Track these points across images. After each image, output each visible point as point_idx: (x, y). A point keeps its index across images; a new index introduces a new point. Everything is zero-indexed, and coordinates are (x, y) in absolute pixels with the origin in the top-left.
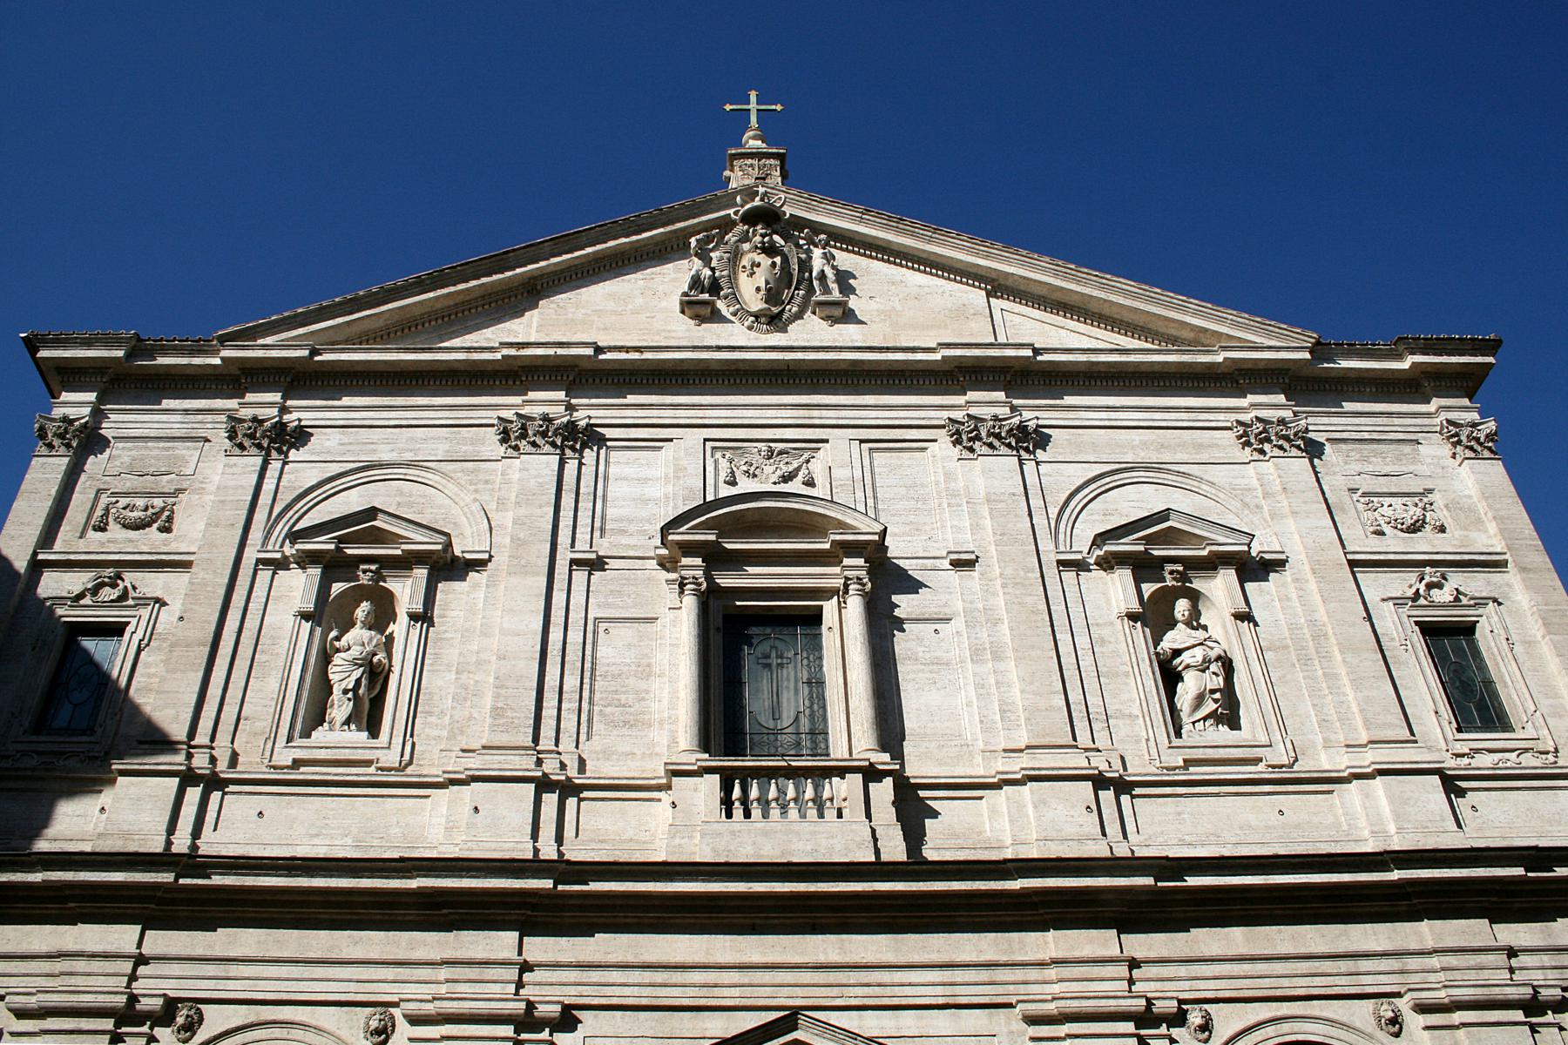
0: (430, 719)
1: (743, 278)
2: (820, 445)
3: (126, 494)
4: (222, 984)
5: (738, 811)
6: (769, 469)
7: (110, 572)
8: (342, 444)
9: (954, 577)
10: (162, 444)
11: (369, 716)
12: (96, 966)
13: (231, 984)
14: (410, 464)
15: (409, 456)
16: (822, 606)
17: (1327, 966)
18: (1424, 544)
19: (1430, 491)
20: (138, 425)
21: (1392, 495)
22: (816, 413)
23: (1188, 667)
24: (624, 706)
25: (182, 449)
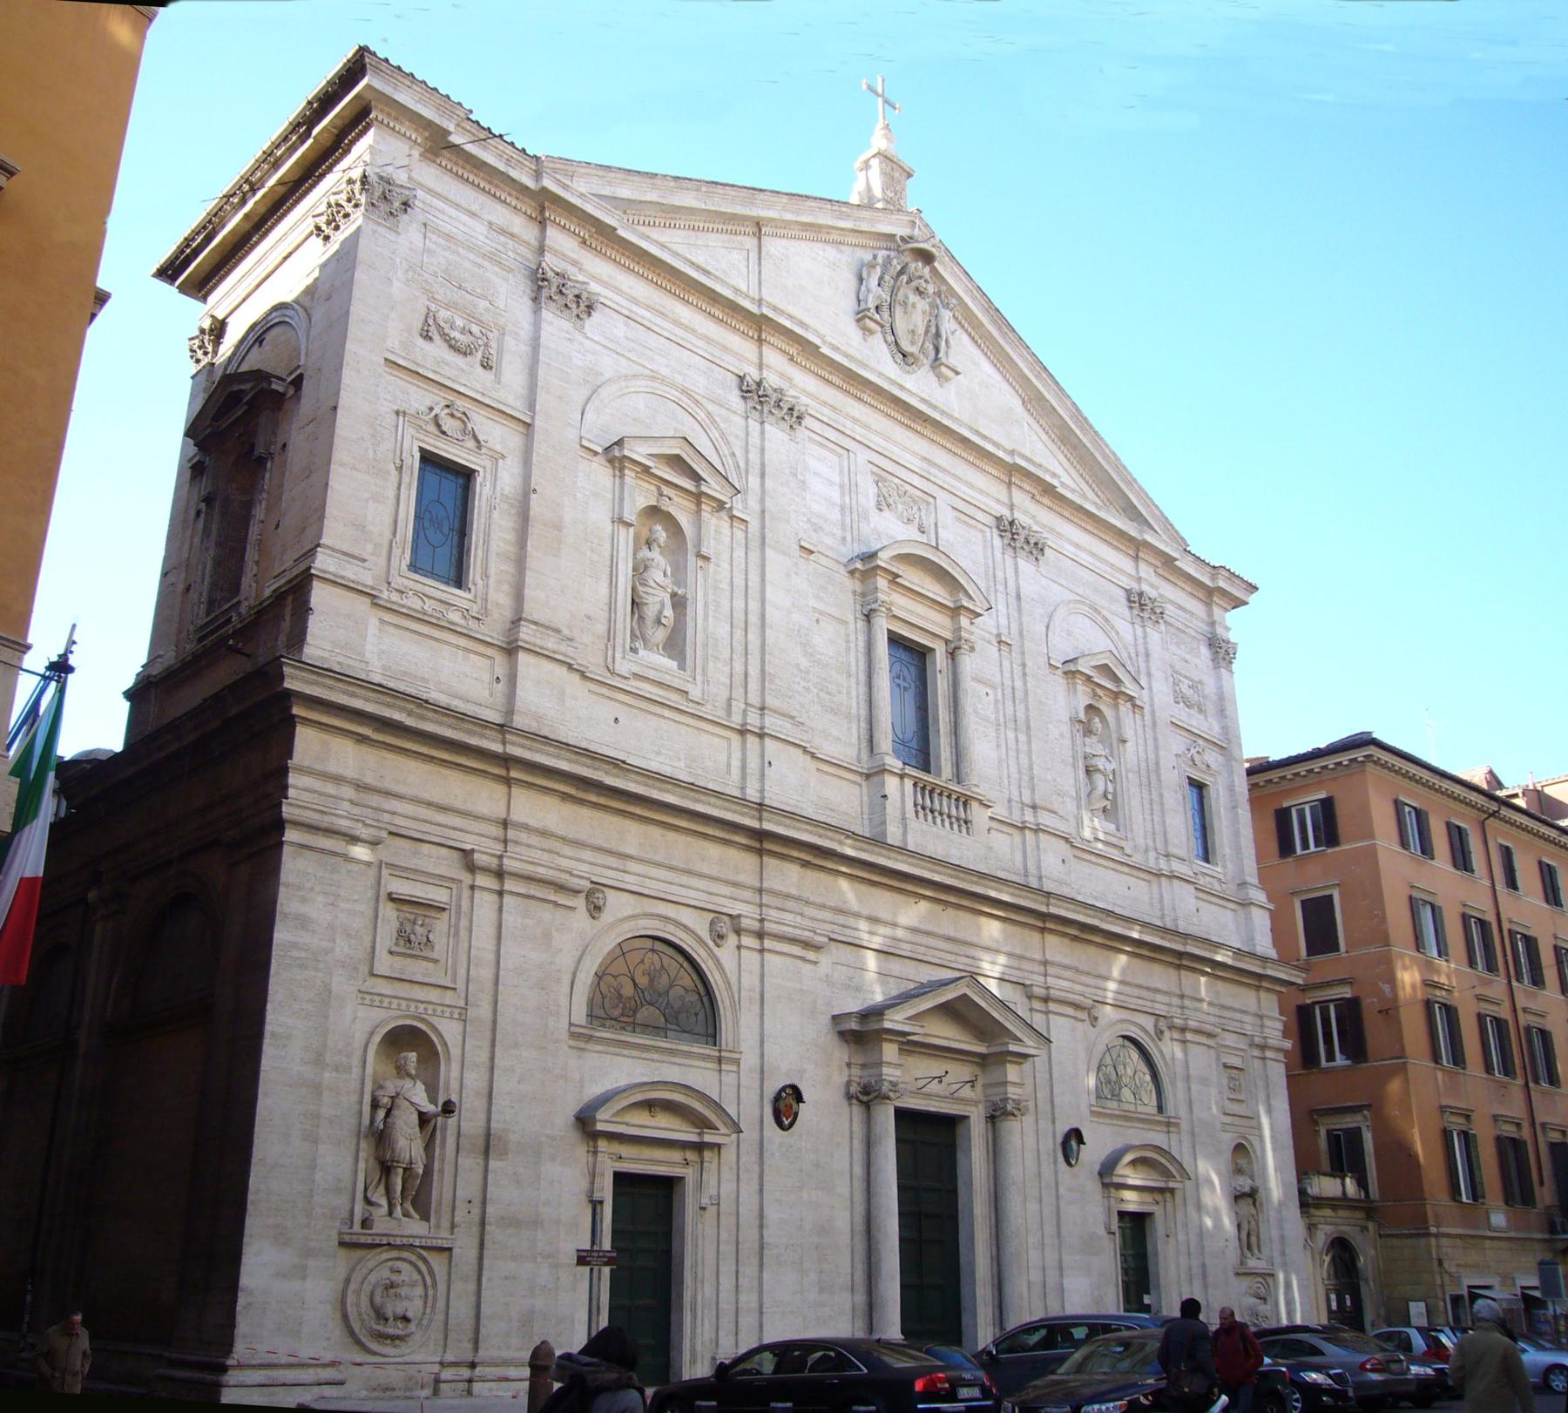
0: (720, 666)
1: (898, 311)
2: (931, 500)
3: (448, 307)
4: (620, 876)
5: (921, 813)
6: (900, 507)
7: (461, 404)
8: (627, 338)
9: (994, 650)
10: (472, 256)
11: (675, 645)
12: (534, 840)
13: (627, 877)
14: (684, 391)
15: (679, 379)
16: (932, 650)
17: (1144, 993)
18: (1195, 721)
19: (1200, 682)
20: (446, 219)
21: (1186, 677)
22: (932, 470)
23: (1099, 770)
24: (828, 693)
25: (492, 273)
